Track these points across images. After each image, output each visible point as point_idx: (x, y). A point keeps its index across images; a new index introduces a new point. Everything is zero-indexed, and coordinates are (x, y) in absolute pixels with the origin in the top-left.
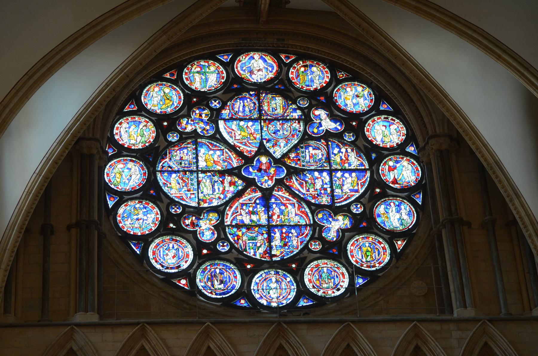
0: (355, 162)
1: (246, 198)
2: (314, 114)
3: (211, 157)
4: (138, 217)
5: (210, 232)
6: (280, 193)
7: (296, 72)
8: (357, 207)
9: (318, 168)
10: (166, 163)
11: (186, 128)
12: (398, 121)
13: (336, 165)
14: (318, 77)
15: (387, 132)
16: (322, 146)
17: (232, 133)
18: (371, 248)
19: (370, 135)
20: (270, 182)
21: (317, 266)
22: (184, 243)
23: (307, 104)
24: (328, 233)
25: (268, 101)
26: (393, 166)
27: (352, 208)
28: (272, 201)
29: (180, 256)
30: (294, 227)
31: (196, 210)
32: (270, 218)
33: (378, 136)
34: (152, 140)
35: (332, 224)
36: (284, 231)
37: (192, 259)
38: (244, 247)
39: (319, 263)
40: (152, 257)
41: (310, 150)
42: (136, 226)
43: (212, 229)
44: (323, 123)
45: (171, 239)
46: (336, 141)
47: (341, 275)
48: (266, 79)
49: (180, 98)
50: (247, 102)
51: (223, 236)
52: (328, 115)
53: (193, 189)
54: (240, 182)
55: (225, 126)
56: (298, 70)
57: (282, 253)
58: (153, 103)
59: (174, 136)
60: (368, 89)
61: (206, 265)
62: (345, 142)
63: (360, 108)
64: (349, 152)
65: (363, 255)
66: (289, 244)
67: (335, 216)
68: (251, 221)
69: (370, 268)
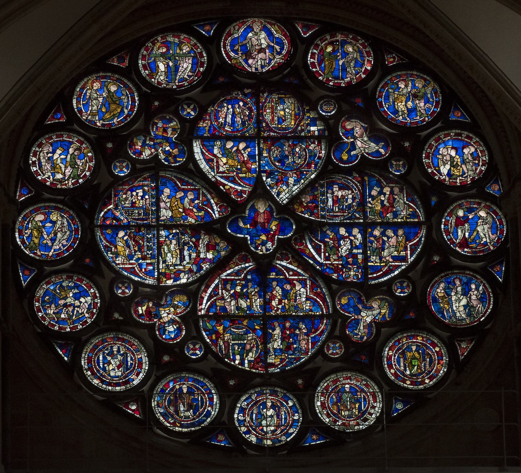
0: (404, 211)
1: (232, 270)
2: (344, 127)
3: (179, 202)
4: (65, 302)
5: (174, 326)
6: (284, 263)
7: (319, 53)
8: (402, 285)
9: (345, 221)
10: (110, 213)
11: (141, 153)
12: (478, 140)
13: (374, 216)
14: (353, 62)
15: (458, 159)
16: (353, 182)
17: (212, 160)
18: (419, 353)
19: (431, 163)
20: (269, 245)
21: (335, 382)
22: (134, 345)
23: (333, 110)
24: (355, 328)
25: (272, 105)
26: (463, 217)
27: (394, 287)
28: (271, 277)
29: (129, 364)
30: (302, 319)
31: (155, 291)
32: (266, 305)
33: (443, 166)
34: (88, 174)
35: (362, 314)
36: (288, 325)
37: (146, 371)
38: (226, 352)
39: (339, 377)
40: (86, 367)
41: (335, 189)
42: (63, 316)
43: (178, 322)
44: (359, 143)
45: (116, 337)
46: (376, 175)
47: (371, 399)
48: (271, 66)
49: (133, 101)
50: (239, 107)
51: (194, 334)
52: (366, 129)
53: (150, 256)
54: (223, 245)
55: (203, 150)
56: (322, 50)
57: (282, 360)
58: (90, 109)
59: (123, 167)
60: (432, 83)
61: (168, 380)
62: (391, 176)
63: (418, 118)
64: (395, 193)
65: (407, 364)
66: (295, 346)
67: (367, 301)
68: (238, 308)
69: (416, 385)
